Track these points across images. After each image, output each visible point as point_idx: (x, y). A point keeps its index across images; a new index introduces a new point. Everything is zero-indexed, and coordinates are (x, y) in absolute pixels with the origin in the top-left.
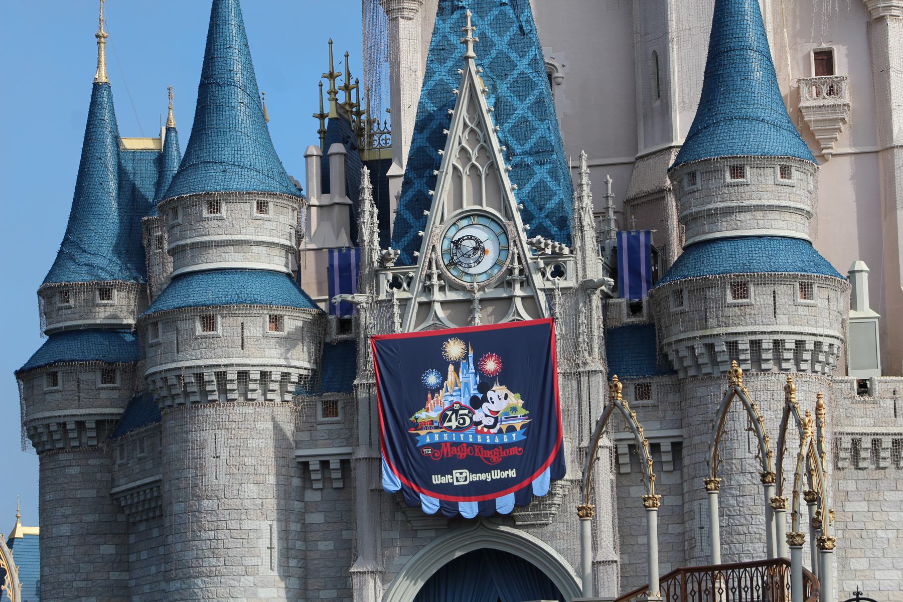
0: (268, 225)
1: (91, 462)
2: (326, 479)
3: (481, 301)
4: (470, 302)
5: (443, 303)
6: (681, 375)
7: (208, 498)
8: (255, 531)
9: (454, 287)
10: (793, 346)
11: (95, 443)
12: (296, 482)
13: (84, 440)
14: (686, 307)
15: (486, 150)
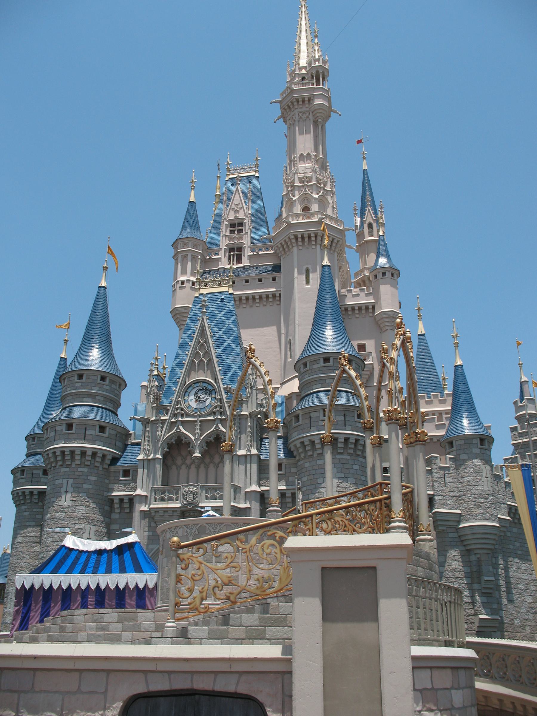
0: (105, 387)
1: (35, 510)
2: (121, 508)
3: (201, 421)
4: (195, 421)
5: (183, 423)
6: (297, 458)
7: (60, 511)
8: (82, 529)
9: (188, 415)
10: (354, 441)
11: (37, 501)
12: (107, 508)
13: (33, 500)
14: (300, 422)
15: (207, 353)
